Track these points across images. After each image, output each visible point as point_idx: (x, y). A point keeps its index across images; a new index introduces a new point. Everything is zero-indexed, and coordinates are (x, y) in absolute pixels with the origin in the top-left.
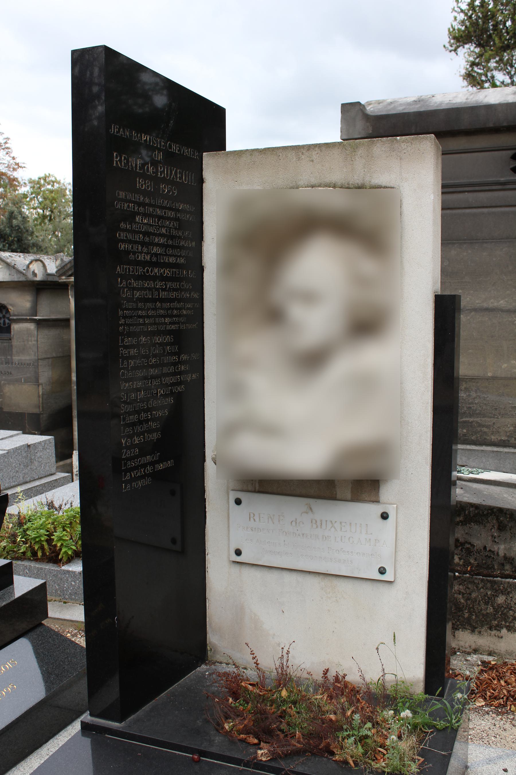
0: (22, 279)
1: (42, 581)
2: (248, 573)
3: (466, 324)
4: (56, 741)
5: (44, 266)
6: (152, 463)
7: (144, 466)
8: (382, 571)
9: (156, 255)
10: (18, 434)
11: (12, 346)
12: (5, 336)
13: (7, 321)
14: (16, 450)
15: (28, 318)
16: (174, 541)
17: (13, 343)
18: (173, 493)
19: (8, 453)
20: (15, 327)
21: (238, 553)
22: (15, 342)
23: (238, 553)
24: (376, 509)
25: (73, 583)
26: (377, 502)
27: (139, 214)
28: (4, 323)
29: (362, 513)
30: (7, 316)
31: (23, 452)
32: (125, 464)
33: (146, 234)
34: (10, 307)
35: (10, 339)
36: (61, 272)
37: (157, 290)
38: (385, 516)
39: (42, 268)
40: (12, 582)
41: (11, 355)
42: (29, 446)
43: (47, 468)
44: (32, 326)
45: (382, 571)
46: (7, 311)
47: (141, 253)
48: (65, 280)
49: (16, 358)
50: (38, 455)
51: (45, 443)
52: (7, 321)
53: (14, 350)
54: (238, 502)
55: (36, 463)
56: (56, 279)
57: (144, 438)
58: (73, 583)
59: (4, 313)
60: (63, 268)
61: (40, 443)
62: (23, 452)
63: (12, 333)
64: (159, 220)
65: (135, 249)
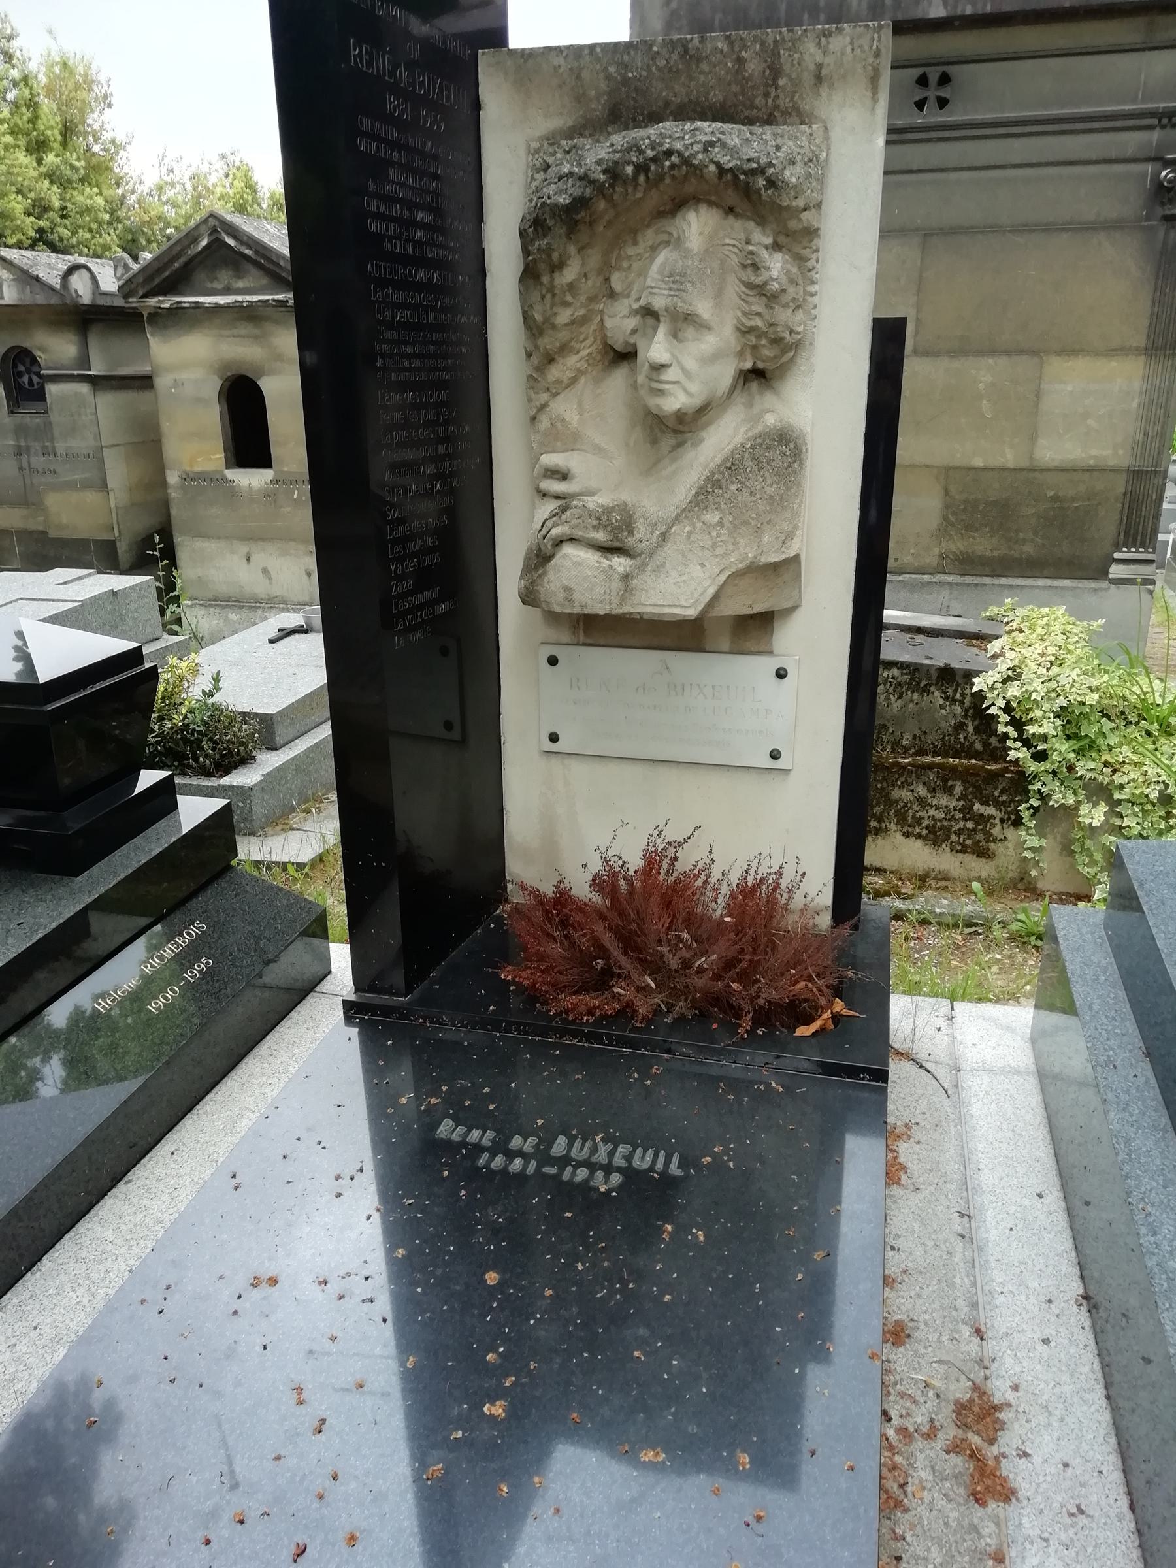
0: (54, 300)
1: (227, 801)
2: (578, 769)
3: (916, 372)
4: (277, 1035)
5: (94, 278)
6: (432, 603)
7: (420, 607)
8: (775, 755)
9: (420, 243)
10: (90, 575)
11: (50, 423)
12: (38, 406)
13: (35, 379)
14: (94, 599)
15: (76, 373)
16: (448, 726)
17: (52, 419)
18: (444, 652)
19: (81, 606)
20: (52, 389)
21: (554, 738)
22: (54, 417)
23: (554, 738)
24: (769, 665)
25: (241, 804)
26: (770, 653)
27: (390, 163)
28: (31, 382)
29: (753, 670)
30: (35, 369)
31: (106, 604)
32: (397, 604)
33: (406, 203)
34: (38, 354)
35: (46, 412)
36: (126, 290)
37: (425, 308)
38: (781, 674)
39: (89, 283)
40: (174, 807)
41: (52, 440)
42: (114, 594)
43: (148, 629)
44: (84, 388)
45: (775, 755)
46: (34, 360)
47: (399, 238)
48: (134, 305)
49: (61, 447)
50: (132, 607)
51: (141, 589)
52: (35, 379)
53: (56, 432)
54: (553, 661)
55: (130, 622)
56: (119, 302)
57: (419, 562)
58: (241, 804)
59: (28, 365)
60: (129, 281)
61: (132, 588)
62: (106, 604)
63: (48, 400)
64: (421, 179)
65: (391, 233)
